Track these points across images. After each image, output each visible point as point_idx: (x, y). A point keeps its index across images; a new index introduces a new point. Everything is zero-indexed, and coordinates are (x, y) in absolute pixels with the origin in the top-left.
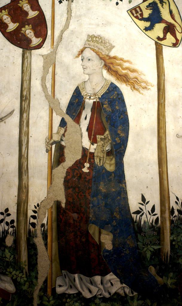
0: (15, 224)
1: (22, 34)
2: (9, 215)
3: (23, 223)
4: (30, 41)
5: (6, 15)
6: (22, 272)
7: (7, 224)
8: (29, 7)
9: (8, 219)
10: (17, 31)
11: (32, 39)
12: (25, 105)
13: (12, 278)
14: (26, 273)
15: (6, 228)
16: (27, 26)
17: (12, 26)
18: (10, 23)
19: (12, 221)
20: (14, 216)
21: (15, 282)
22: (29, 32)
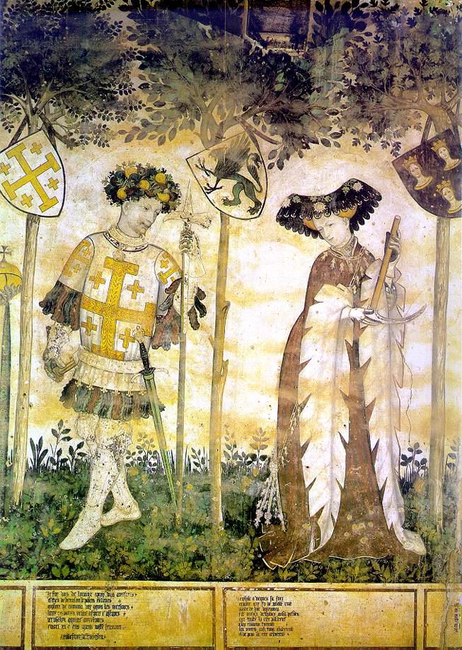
0: (427, 464)
1: (437, 193)
2: (419, 452)
3: (437, 462)
4: (446, 204)
5: (414, 163)
6: (436, 528)
7: (417, 464)
8: (447, 152)
9: (418, 458)
10: (431, 188)
11: (451, 202)
12: (441, 297)
13: (422, 536)
14: (440, 529)
15: (416, 469)
16: (443, 182)
17: (423, 181)
18: (419, 177)
19: (424, 461)
20: (425, 454)
21: (425, 540)
22: (447, 192)
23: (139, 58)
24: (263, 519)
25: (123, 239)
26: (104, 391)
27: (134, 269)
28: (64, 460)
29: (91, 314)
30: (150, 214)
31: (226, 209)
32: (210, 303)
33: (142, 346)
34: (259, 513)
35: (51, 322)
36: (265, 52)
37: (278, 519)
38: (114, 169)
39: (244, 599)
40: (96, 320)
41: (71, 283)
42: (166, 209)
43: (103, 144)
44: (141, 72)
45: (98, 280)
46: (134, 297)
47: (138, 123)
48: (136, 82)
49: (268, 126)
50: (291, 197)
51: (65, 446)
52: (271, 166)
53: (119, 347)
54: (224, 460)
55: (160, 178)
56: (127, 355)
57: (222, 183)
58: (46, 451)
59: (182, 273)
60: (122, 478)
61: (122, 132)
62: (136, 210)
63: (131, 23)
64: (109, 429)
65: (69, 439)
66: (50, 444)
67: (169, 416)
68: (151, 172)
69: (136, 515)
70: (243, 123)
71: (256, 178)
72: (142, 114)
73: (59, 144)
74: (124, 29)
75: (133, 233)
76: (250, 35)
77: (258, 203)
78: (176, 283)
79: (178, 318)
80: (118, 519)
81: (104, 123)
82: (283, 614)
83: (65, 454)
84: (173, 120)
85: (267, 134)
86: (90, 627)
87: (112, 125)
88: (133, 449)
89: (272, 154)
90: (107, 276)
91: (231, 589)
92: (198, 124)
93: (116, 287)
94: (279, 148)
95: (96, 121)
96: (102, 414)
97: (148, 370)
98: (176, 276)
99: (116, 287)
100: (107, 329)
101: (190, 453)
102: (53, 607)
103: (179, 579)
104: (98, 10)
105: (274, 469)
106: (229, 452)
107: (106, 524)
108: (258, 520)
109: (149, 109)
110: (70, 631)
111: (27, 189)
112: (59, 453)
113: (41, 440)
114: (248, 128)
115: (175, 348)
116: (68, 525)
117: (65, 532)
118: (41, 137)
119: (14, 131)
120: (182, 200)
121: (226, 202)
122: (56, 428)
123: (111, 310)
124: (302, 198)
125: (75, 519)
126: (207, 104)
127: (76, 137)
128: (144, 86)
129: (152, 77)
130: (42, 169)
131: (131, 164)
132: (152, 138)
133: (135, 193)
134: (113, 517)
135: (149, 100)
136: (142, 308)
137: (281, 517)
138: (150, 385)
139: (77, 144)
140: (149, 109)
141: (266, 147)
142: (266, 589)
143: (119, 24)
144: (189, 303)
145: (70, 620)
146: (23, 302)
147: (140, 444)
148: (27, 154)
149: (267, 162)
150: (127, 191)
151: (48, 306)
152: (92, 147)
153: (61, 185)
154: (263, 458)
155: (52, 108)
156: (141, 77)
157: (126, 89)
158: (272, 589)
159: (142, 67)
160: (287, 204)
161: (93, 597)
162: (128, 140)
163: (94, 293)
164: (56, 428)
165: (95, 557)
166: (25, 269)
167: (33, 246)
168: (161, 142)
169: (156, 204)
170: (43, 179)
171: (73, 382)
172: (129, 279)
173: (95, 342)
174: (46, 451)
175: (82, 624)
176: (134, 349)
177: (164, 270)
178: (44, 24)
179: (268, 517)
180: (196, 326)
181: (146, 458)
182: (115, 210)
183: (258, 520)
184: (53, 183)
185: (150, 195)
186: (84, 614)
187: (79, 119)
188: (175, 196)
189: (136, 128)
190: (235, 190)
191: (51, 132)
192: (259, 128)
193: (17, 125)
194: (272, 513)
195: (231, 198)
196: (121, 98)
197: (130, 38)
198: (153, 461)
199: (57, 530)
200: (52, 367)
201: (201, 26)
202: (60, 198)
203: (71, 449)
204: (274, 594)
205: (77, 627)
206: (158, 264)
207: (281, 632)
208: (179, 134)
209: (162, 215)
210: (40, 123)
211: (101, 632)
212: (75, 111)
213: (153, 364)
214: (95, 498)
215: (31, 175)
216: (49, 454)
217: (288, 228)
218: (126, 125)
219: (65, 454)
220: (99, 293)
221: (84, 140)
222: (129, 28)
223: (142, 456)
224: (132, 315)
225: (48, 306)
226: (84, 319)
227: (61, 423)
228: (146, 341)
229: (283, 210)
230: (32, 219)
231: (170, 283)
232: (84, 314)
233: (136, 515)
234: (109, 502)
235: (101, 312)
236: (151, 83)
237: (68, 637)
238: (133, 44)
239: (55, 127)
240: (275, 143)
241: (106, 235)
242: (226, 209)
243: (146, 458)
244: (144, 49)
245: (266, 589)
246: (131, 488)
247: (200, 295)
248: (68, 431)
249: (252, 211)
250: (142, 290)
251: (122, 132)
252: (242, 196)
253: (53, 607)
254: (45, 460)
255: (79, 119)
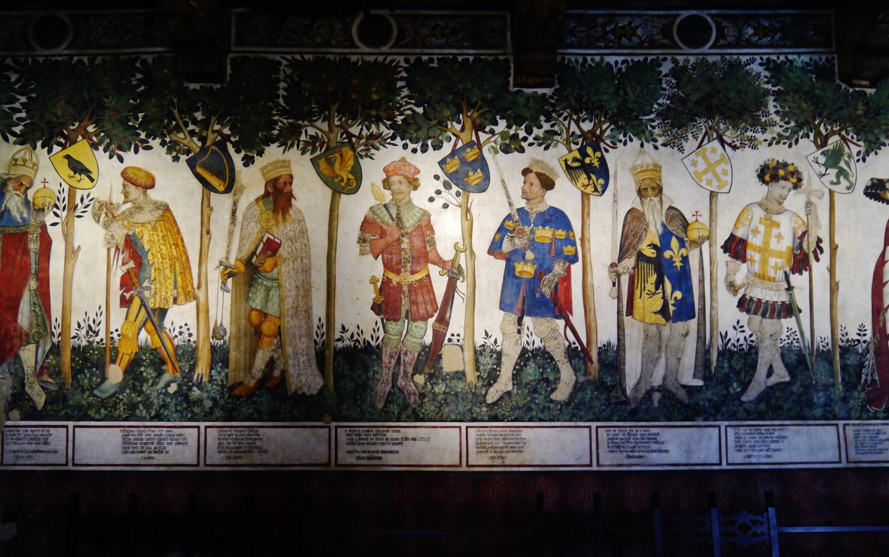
23: (772, 95)
24: (866, 380)
25: (770, 206)
26: (764, 301)
27: (778, 225)
28: (741, 345)
29: (753, 254)
30: (785, 191)
31: (833, 187)
32: (825, 245)
33: (786, 273)
34: (863, 377)
35: (729, 259)
36: (851, 90)
37: (875, 380)
38: (762, 163)
39: (857, 430)
40: (757, 257)
41: (740, 234)
42: (796, 186)
43: (754, 147)
44: (775, 103)
45: (755, 232)
46: (778, 242)
47: (775, 135)
48: (772, 110)
49: (855, 136)
50: (872, 179)
51: (741, 336)
52: (858, 161)
53: (772, 275)
54: (840, 343)
55: (791, 168)
56: (777, 279)
57: (829, 171)
58: (730, 340)
59: (808, 227)
60: (778, 356)
61: (766, 140)
62: (779, 188)
63: (768, 74)
64: (769, 325)
65: (743, 331)
66: (732, 335)
67: (805, 317)
68: (785, 165)
69: (788, 379)
70: (840, 134)
71: (849, 166)
72: (777, 129)
73: (727, 147)
74: (762, 77)
75: (776, 203)
76: (841, 80)
77: (851, 184)
78: (804, 234)
79: (806, 256)
80: (776, 382)
81: (754, 135)
82: (881, 440)
83: (742, 341)
84: (797, 133)
85: (855, 141)
86: (762, 450)
87: (760, 136)
88: (784, 337)
89: (858, 153)
90: (762, 229)
91: (848, 424)
92: (812, 135)
93: (767, 235)
94: (863, 149)
95: (749, 134)
96: (764, 315)
97: (790, 288)
98: (804, 229)
99: (767, 235)
100: (764, 262)
101: (819, 339)
102: (738, 438)
103: (815, 419)
104: (746, 66)
105: (872, 347)
106: (843, 338)
107: (769, 384)
108: (863, 381)
109: (781, 126)
110: (750, 453)
111: (710, 176)
112: (738, 340)
113: (726, 333)
114: (843, 138)
115: (806, 274)
116: (745, 386)
117: (744, 390)
118: (716, 144)
119: (699, 140)
120: (805, 182)
121: (832, 183)
122: (736, 325)
123: (764, 250)
124: (878, 180)
125: (750, 381)
126: (817, 122)
127: (738, 144)
128: (777, 113)
129: (781, 106)
130: (718, 162)
131: (772, 160)
132: (785, 143)
133: (775, 178)
134: (773, 380)
135: (781, 120)
136: (784, 250)
137: (877, 378)
138: (791, 296)
139: (738, 148)
140: (781, 126)
141: (855, 149)
142: (870, 425)
143: (759, 74)
144: (813, 246)
145: (750, 446)
146: (710, 246)
147: (788, 334)
148: (708, 153)
149: (856, 158)
150: (771, 177)
151: (726, 248)
152: (747, 150)
153: (729, 173)
154: (865, 342)
155: (722, 126)
156: (775, 106)
157: (767, 114)
158: (874, 425)
159: (774, 101)
160: (870, 184)
161: (763, 431)
162: (770, 145)
163: (754, 239)
164: (736, 325)
165: (762, 406)
166: (710, 226)
167: (714, 211)
168: (790, 146)
169: (789, 185)
170: (719, 170)
171: (744, 295)
172: (775, 231)
173: (757, 271)
174: (730, 340)
175: (757, 448)
176: (780, 275)
177: (796, 226)
178: (713, 74)
179: (869, 378)
180: (817, 260)
181: (792, 343)
182: (765, 188)
183: (863, 381)
184: (725, 172)
185: (785, 179)
186: (758, 442)
187: (739, 133)
188: (800, 180)
189: (774, 138)
190: (838, 176)
191: (723, 142)
192: (849, 137)
193: (701, 137)
194: (872, 375)
195: (835, 180)
196: (763, 120)
197: (767, 83)
198: (797, 345)
199: (739, 390)
200: (732, 287)
201: (810, 75)
202: (730, 182)
203: (745, 338)
204: (876, 428)
205: (754, 451)
206: (793, 222)
207: (881, 451)
208: (800, 140)
209: (793, 192)
210: (715, 135)
211: (769, 453)
212: (735, 127)
213: (792, 284)
214: (762, 370)
215: (710, 167)
216: (732, 341)
217: (871, 198)
218: (768, 136)
219: (742, 341)
220: (755, 241)
221: (743, 145)
222: (766, 77)
223: (789, 341)
224: (779, 254)
225: (726, 248)
226: (748, 257)
227: (738, 322)
228: (787, 269)
229: (867, 188)
230: (713, 195)
231: (800, 233)
232: (749, 253)
233: (788, 379)
234: (771, 370)
235: (759, 251)
236: (781, 110)
237: (749, 456)
238: (769, 86)
239: (725, 138)
240: (859, 146)
241: (760, 205)
242: (833, 187)
243: (792, 343)
244: (776, 89)
245: (870, 425)
246: (783, 361)
247: (819, 240)
248: (742, 327)
249: (848, 188)
250: (783, 238)
251: (766, 140)
252: (842, 178)
253: (738, 438)
254: (729, 345)
255: (739, 133)
